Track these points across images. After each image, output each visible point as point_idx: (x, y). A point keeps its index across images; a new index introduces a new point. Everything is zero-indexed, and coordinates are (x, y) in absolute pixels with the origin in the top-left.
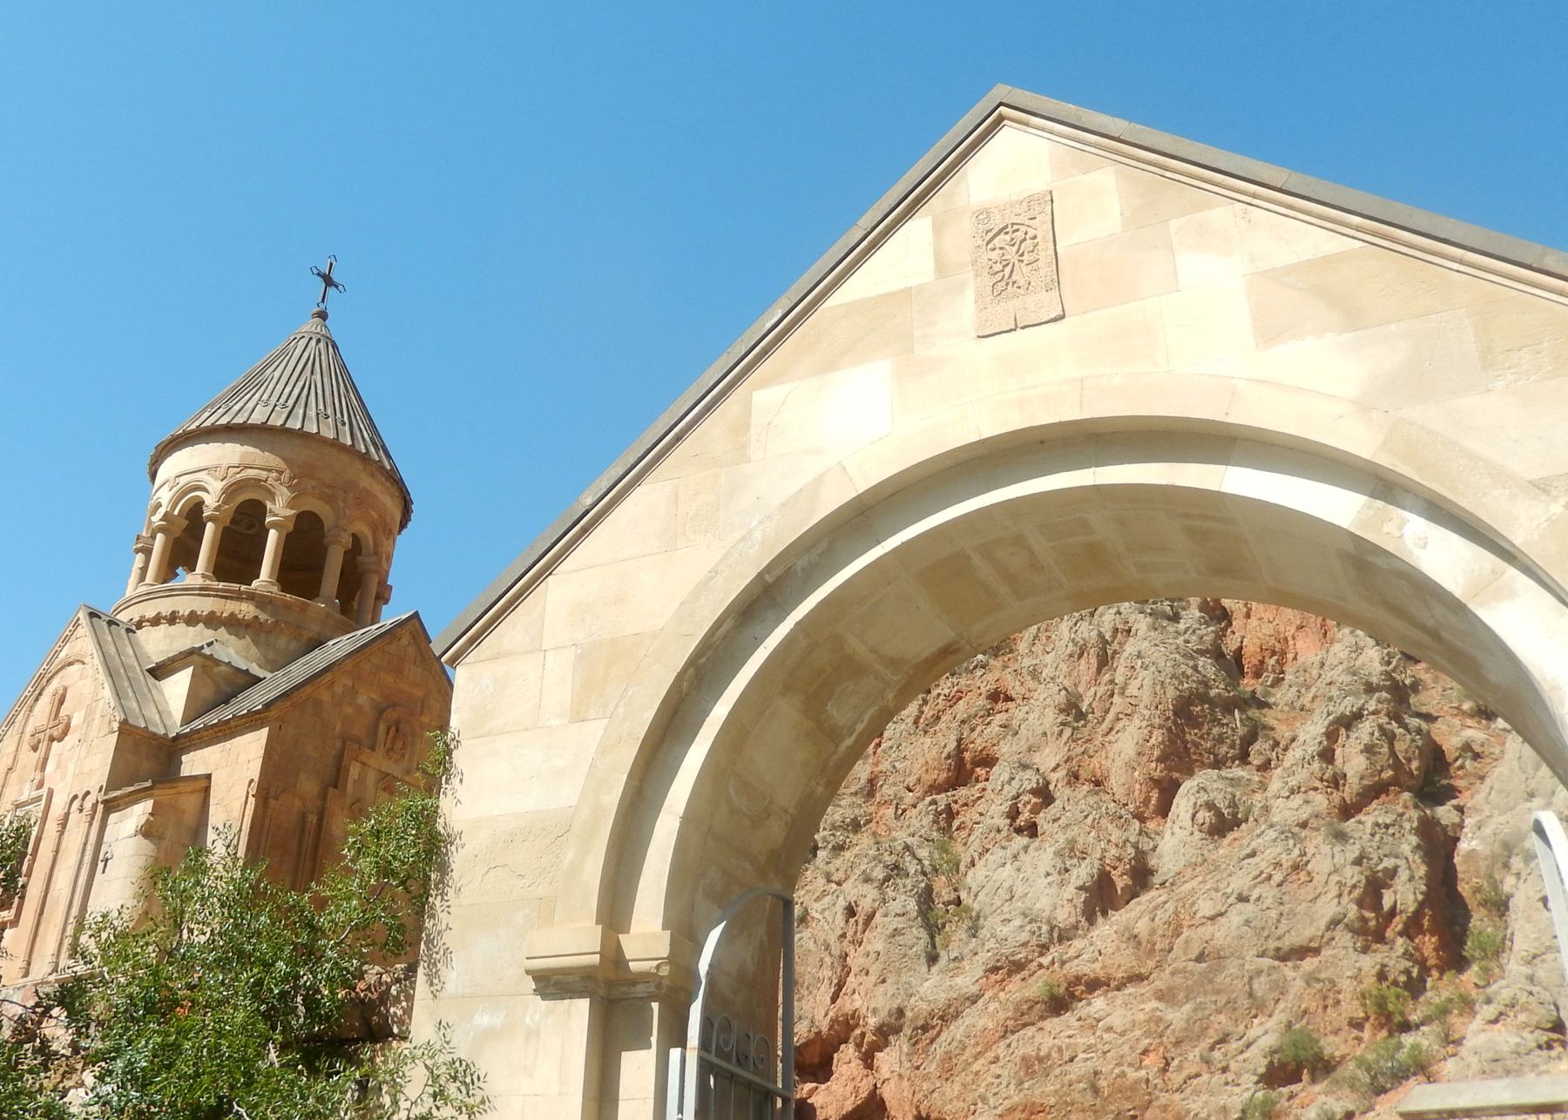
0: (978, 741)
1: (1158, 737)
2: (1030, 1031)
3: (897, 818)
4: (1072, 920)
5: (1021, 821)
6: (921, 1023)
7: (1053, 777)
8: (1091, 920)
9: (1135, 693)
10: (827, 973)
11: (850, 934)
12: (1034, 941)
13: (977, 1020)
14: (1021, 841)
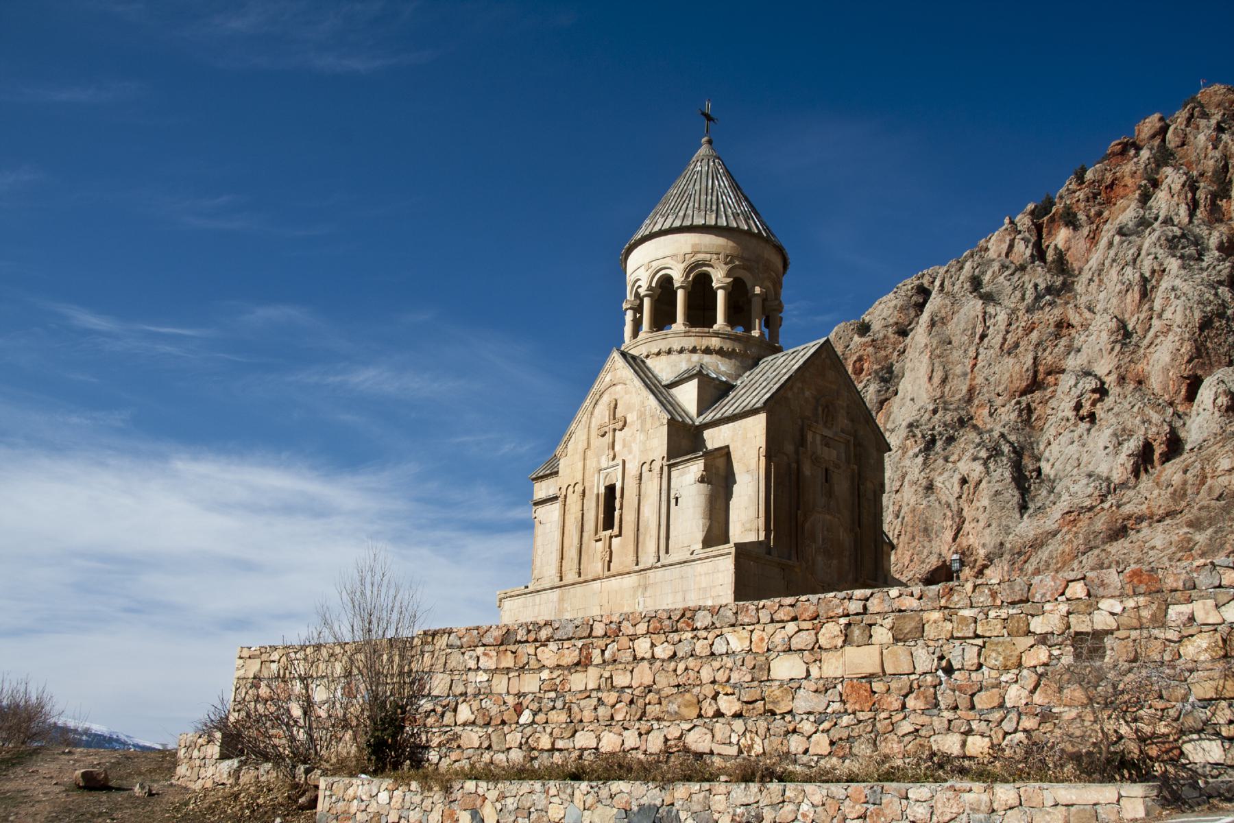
0: (1049, 358)
1: (1187, 348)
2: (1096, 552)
3: (991, 415)
4: (1124, 477)
5: (1084, 412)
7: (1108, 380)
8: (1137, 476)
9: (1170, 316)
10: (949, 522)
11: (964, 497)
12: (1097, 493)
13: (1055, 547)
14: (1084, 426)
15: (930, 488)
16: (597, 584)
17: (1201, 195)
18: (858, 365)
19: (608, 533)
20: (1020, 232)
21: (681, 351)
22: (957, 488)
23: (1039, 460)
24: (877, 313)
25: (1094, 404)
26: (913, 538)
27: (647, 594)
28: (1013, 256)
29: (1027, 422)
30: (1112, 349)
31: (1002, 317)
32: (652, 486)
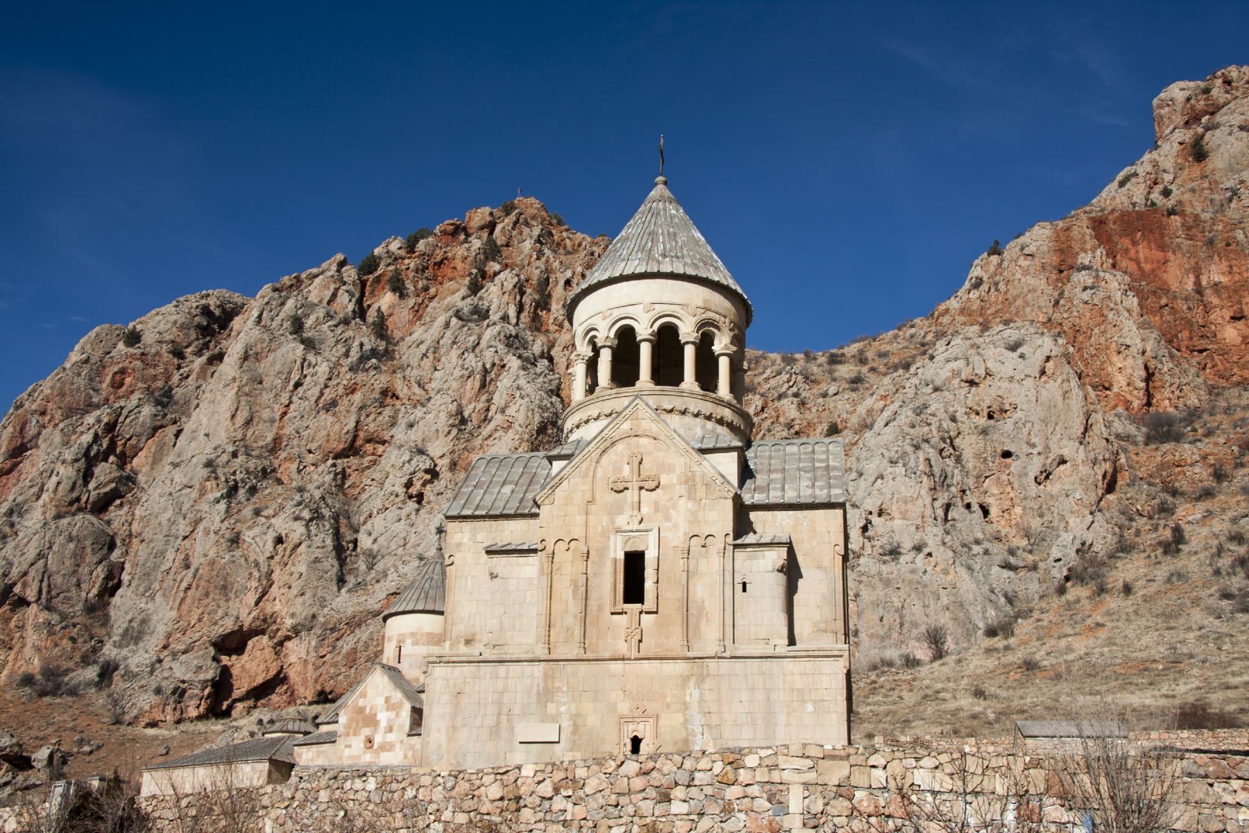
0: (372, 425)
3: (299, 471)
5: (413, 491)
7: (440, 462)
10: (254, 584)
11: (277, 558)
14: (412, 505)
15: (235, 541)
16: (616, 667)
17: (527, 300)
18: (118, 377)
19: (639, 606)
20: (345, 283)
21: (697, 415)
22: (270, 546)
23: (357, 531)
24: (151, 324)
25: (424, 485)
26: (207, 595)
27: (706, 686)
28: (336, 306)
29: (341, 487)
30: (449, 433)
31: (323, 369)
32: (711, 565)
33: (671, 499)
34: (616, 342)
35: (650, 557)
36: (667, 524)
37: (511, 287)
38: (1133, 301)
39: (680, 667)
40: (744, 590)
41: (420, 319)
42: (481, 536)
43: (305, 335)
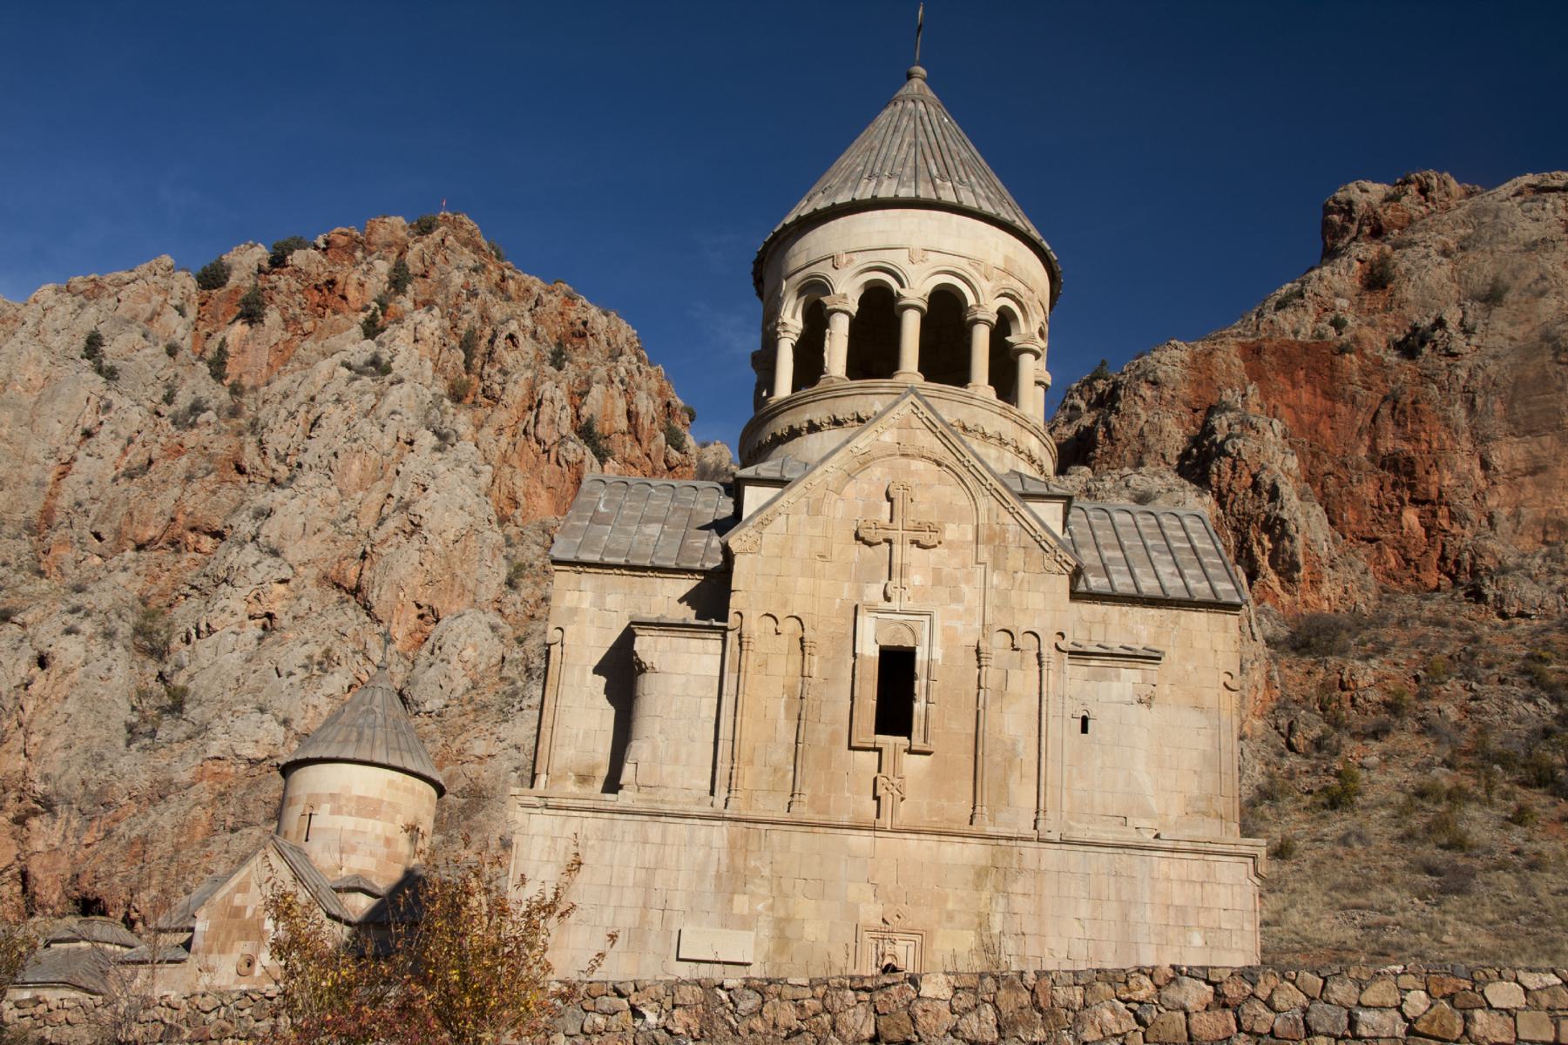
6: (106, 800)
11: (35, 688)
12: (267, 740)
19: (903, 740)
27: (1017, 888)
33: (964, 566)
34: (854, 308)
35: (921, 657)
36: (954, 606)
37: (427, 333)
38: (1293, 463)
39: (973, 852)
40: (1084, 729)
41: (285, 363)
42: (612, 601)
43: (106, 363)
